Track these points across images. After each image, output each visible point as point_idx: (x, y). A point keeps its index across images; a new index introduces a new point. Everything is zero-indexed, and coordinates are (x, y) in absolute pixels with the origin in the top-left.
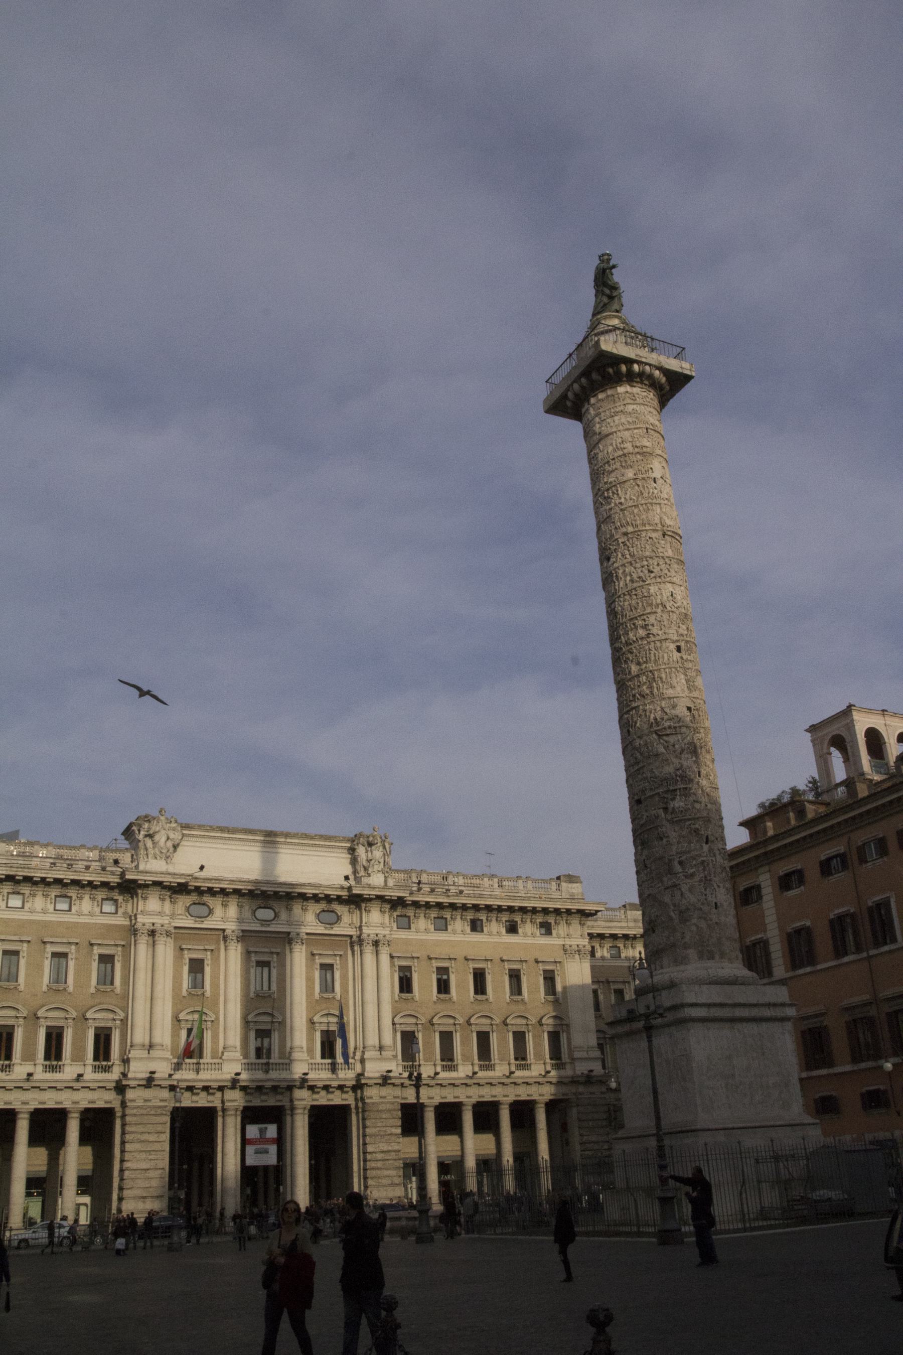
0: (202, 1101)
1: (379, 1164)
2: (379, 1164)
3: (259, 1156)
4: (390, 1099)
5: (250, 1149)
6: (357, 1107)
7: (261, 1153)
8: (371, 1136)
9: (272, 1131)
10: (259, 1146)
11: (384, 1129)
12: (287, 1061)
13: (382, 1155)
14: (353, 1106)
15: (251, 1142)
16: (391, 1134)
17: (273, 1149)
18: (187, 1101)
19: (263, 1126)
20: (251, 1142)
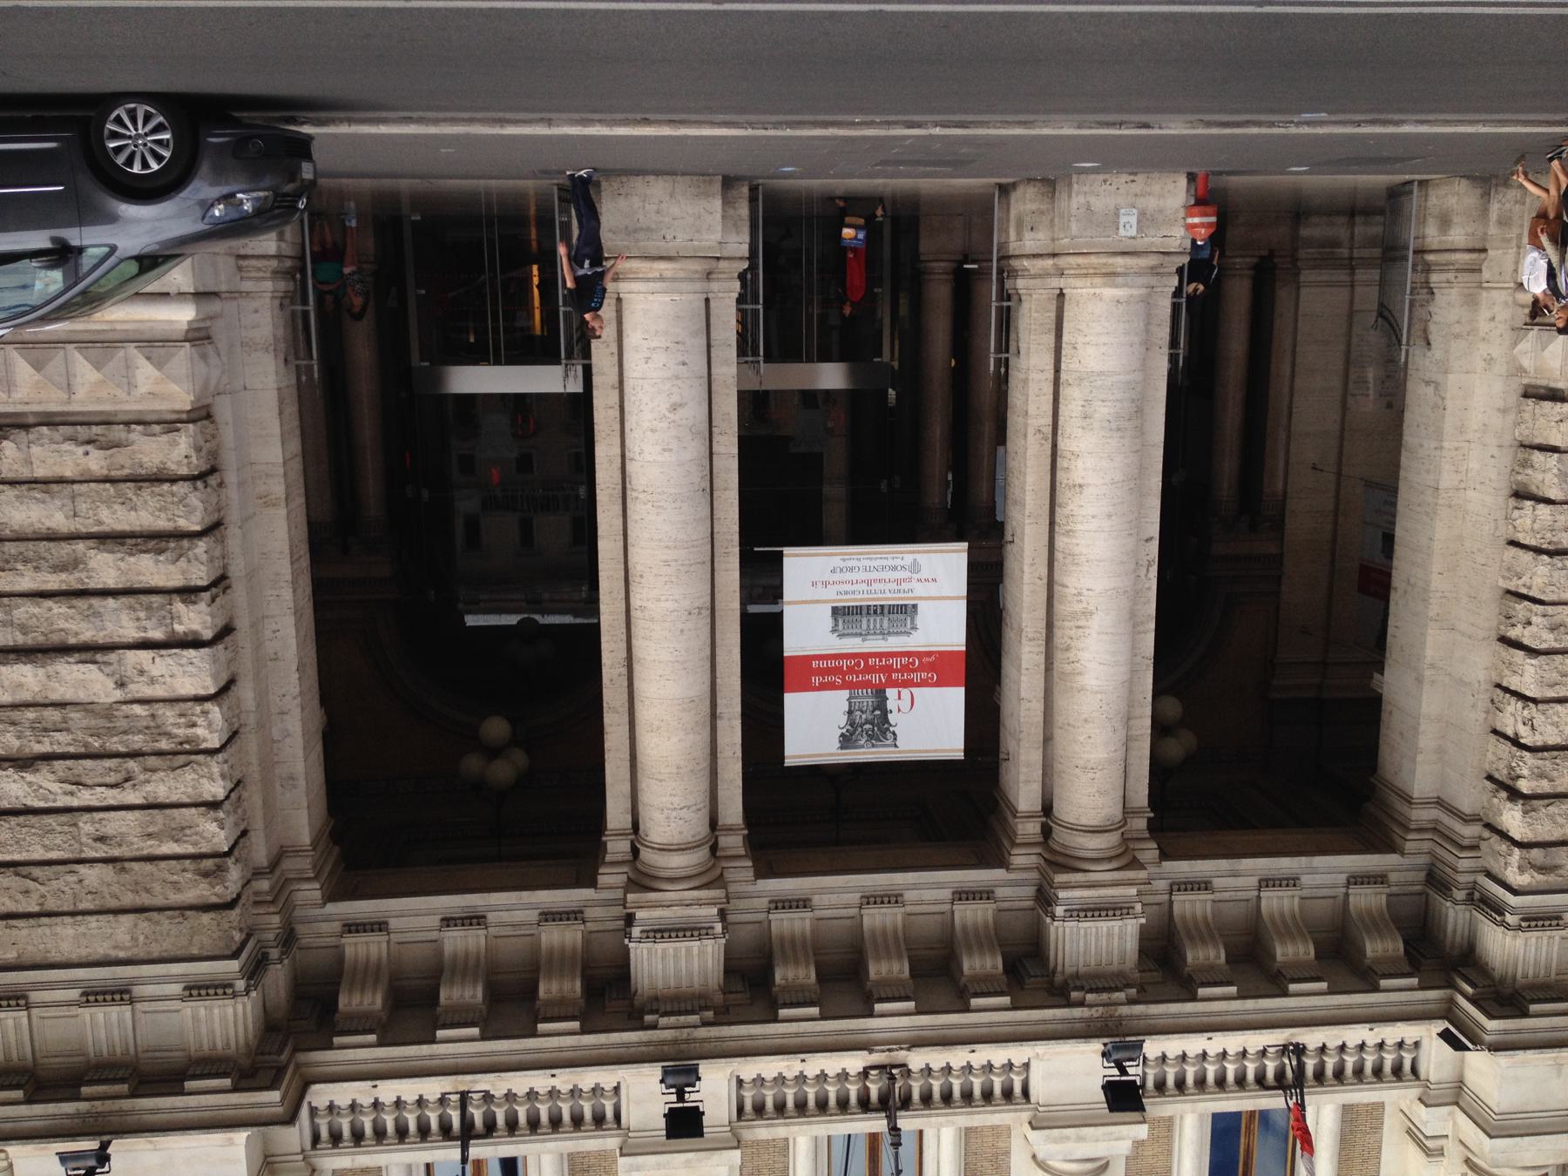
0: (1234, 880)
1: (106, 568)
2: (106, 568)
3: (886, 595)
4: (53, 990)
5: (944, 626)
6: (281, 896)
7: (879, 611)
8: (188, 753)
9: (813, 728)
10: (894, 643)
11: (85, 797)
12: (762, 1132)
13: (88, 634)
14: (310, 892)
15: (934, 668)
16: (24, 763)
17: (807, 630)
18: (1324, 874)
19: (866, 754)
20: (934, 668)
